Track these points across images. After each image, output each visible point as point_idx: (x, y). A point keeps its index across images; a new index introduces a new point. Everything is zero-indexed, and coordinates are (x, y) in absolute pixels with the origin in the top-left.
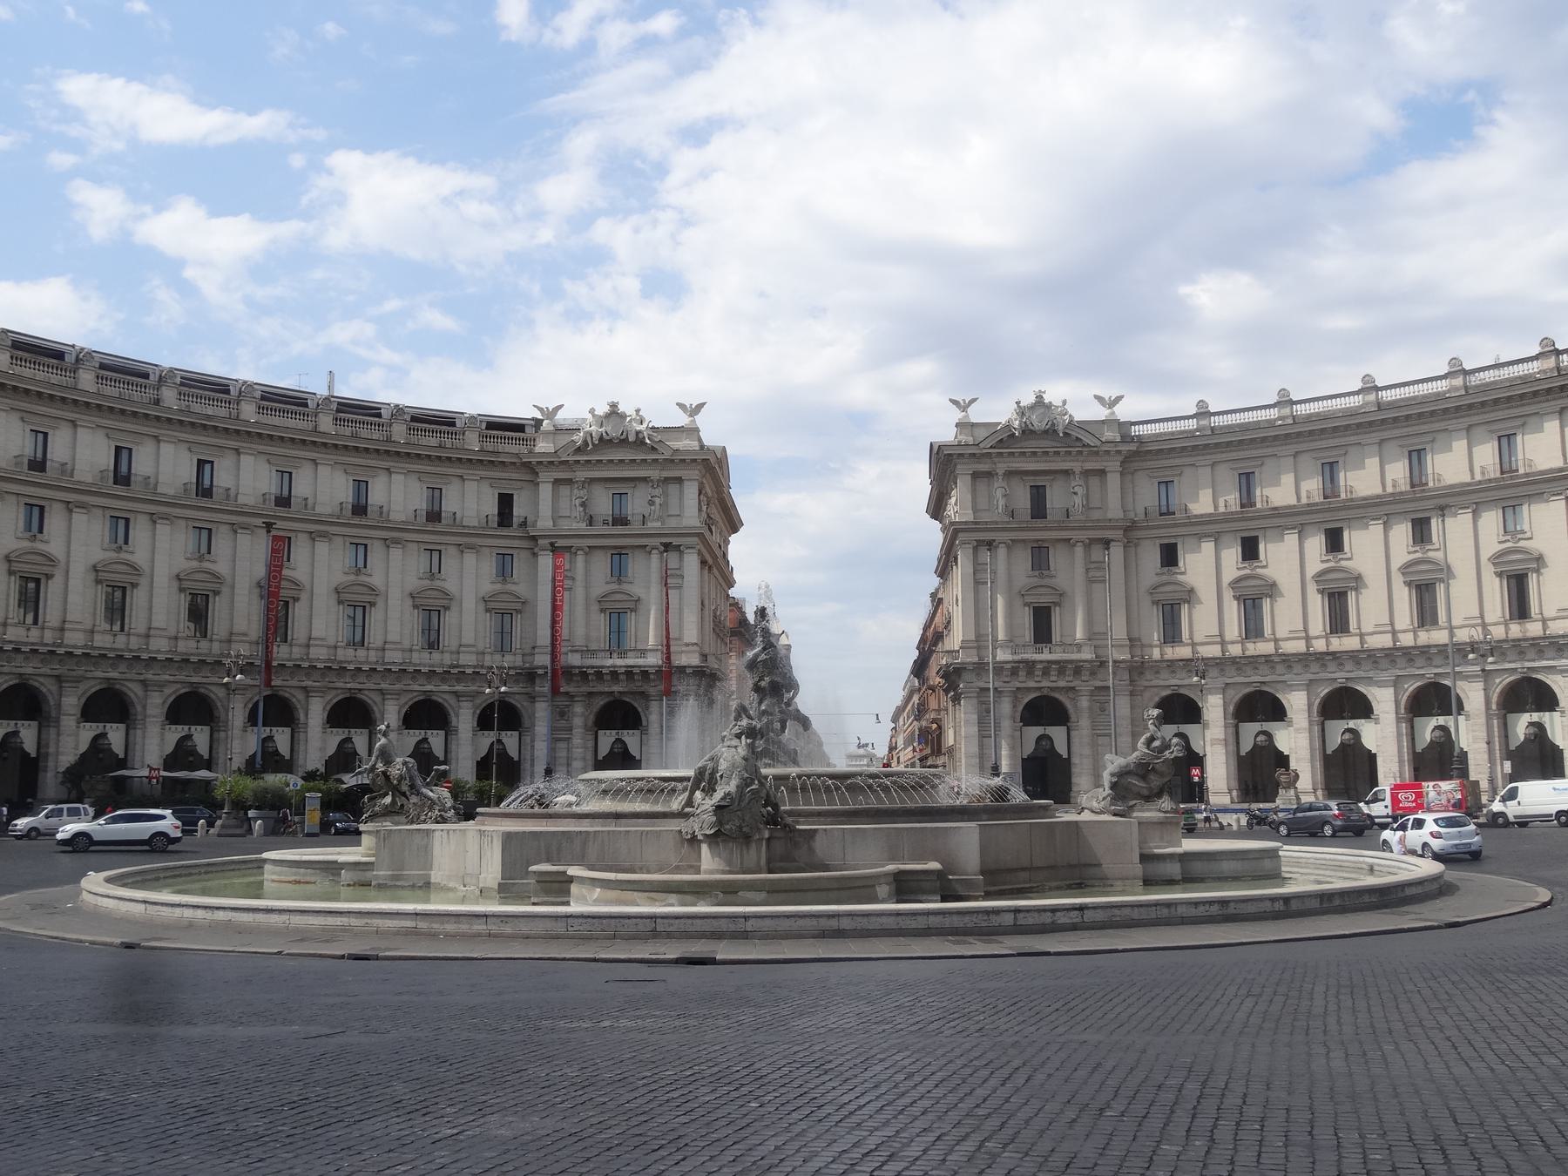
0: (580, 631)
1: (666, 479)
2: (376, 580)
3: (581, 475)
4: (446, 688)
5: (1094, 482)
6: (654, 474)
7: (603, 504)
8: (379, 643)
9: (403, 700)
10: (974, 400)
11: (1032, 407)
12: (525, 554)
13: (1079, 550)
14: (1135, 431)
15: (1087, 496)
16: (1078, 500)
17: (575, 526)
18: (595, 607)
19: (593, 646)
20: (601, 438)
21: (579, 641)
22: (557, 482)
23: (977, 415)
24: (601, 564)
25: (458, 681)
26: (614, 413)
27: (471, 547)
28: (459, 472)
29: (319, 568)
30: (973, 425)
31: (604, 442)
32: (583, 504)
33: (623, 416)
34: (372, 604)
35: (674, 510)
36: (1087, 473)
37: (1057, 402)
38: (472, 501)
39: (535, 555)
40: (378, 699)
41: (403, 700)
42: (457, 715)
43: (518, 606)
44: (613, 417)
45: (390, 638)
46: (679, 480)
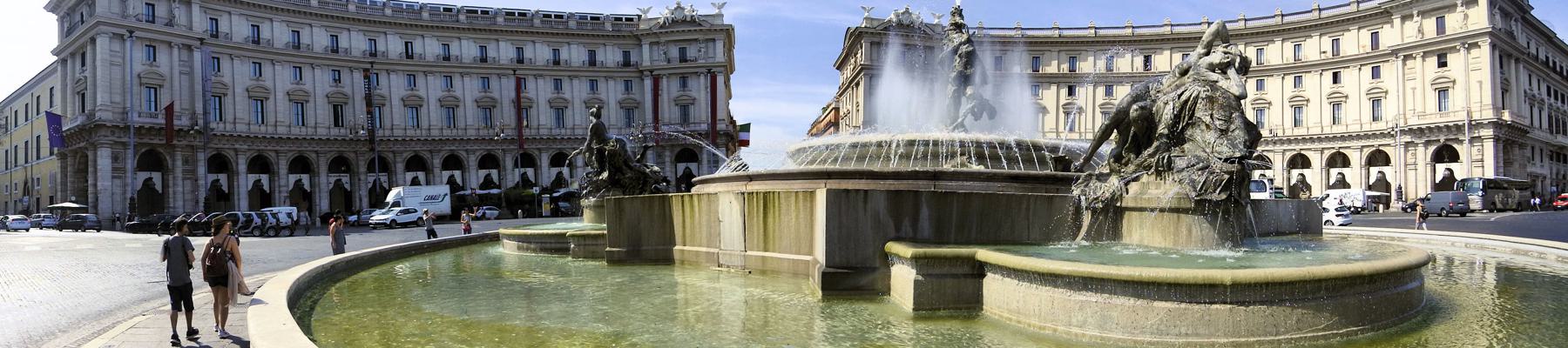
0: (666, 116)
2: (567, 96)
3: (663, 39)
29: (540, 91)
31: (674, 22)
38: (610, 56)
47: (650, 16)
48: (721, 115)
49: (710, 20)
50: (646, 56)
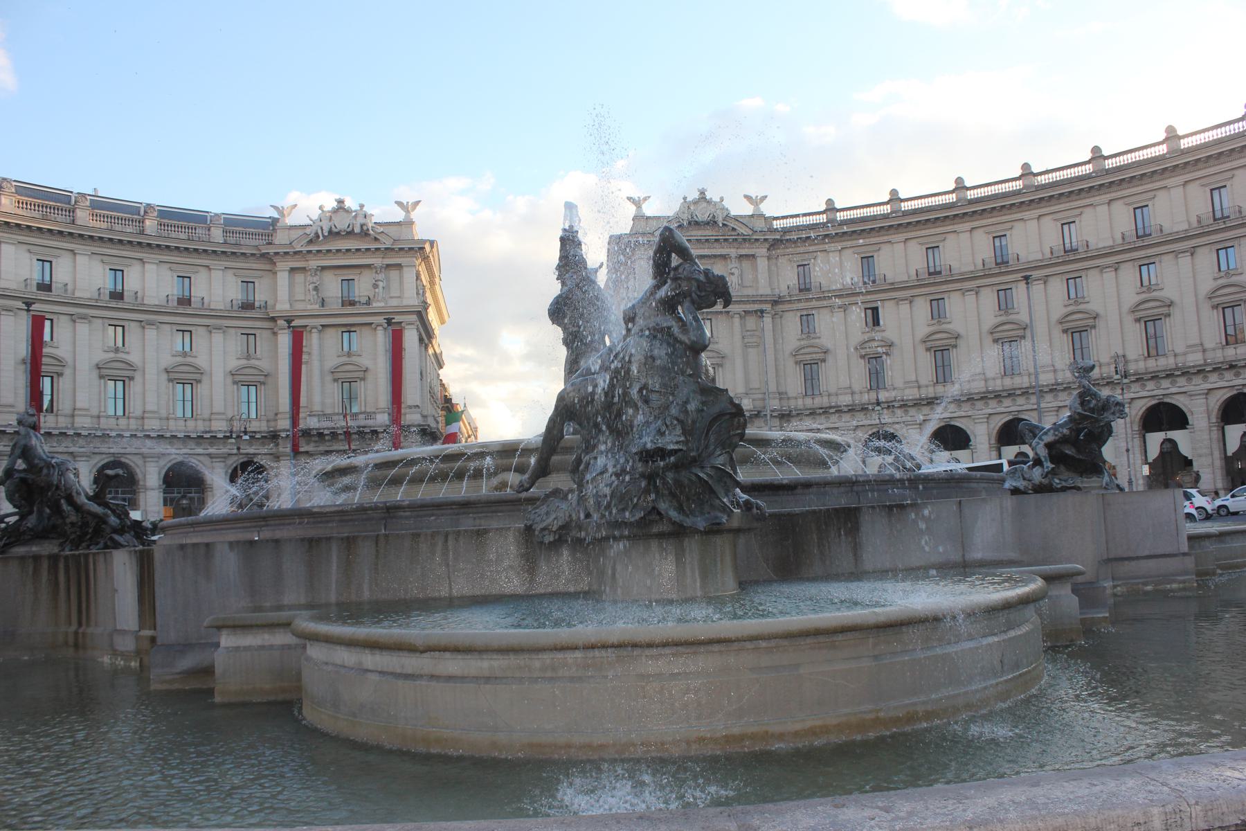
0: (317, 398)
1: (388, 266)
2: (134, 358)
4: (200, 451)
5: (746, 264)
6: (377, 261)
7: (332, 286)
8: (138, 413)
9: (162, 462)
10: (645, 199)
11: (695, 202)
12: (266, 334)
13: (737, 320)
14: (777, 224)
15: (741, 275)
17: (309, 307)
18: (329, 378)
19: (328, 411)
20: (330, 232)
21: (317, 408)
22: (293, 270)
23: (649, 210)
25: (212, 445)
29: (78, 345)
30: (648, 218)
32: (316, 289)
33: (348, 211)
34: (131, 378)
39: (275, 334)
40: (140, 462)
41: (162, 462)
43: (262, 379)
44: (341, 213)
45: (149, 407)
46: (399, 266)
47: (290, 221)
48: (411, 394)
49: (392, 231)
50: (283, 292)
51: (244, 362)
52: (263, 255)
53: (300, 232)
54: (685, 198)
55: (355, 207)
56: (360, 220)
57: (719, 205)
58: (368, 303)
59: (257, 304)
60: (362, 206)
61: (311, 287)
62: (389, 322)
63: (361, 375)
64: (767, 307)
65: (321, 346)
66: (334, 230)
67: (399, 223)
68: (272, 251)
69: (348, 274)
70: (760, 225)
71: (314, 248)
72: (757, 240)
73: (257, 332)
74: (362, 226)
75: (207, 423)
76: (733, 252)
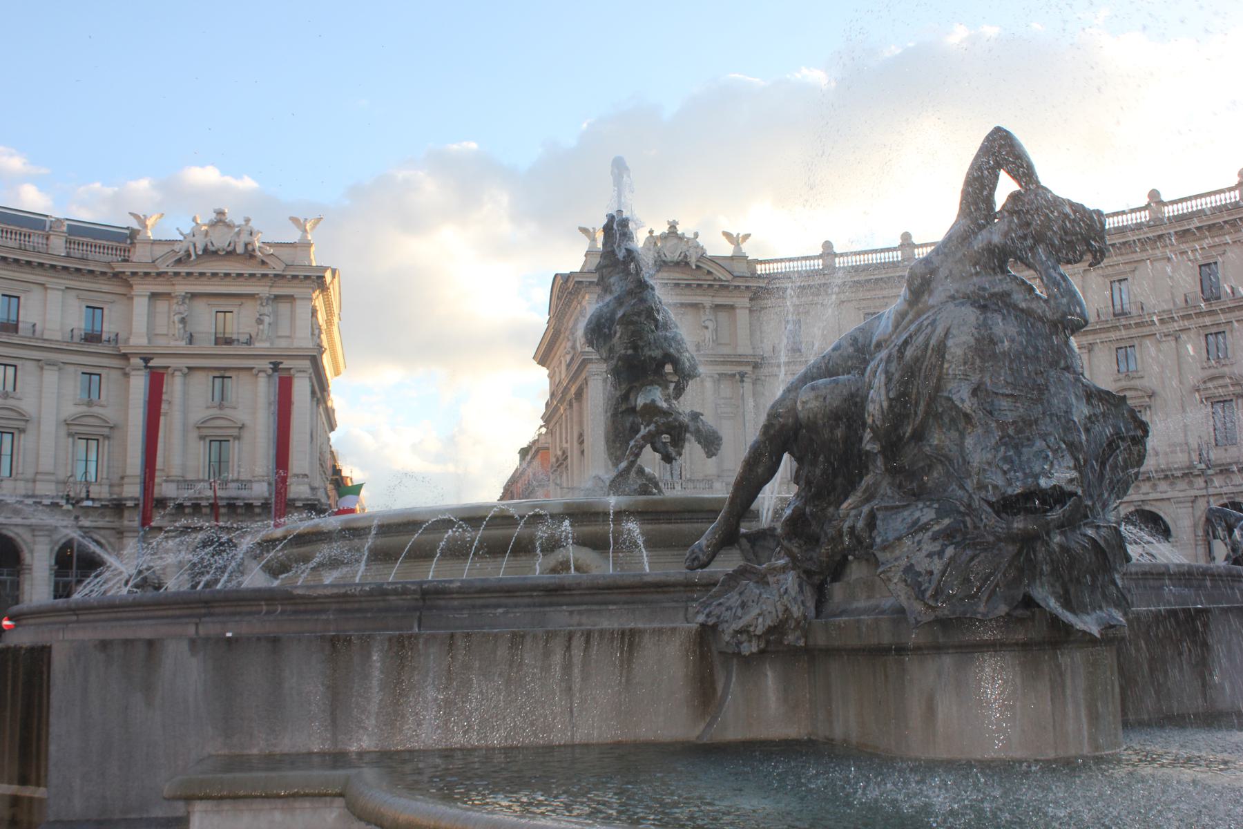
0: (176, 460)
1: (277, 297)
4: (18, 520)
5: (723, 316)
6: (263, 290)
11: (664, 237)
12: (115, 375)
13: (709, 384)
14: (761, 269)
16: (708, 334)
17: (173, 343)
18: (194, 435)
19: (191, 476)
20: (205, 250)
21: (176, 472)
22: (154, 296)
24: (201, 386)
26: (220, 220)
27: (52, 364)
28: (41, 279)
32: (183, 321)
33: (229, 226)
35: (284, 330)
36: (718, 307)
37: (690, 235)
39: (126, 375)
42: (32, 551)
43: (106, 431)
44: (220, 227)
46: (291, 298)
48: (299, 460)
49: (285, 254)
50: (139, 322)
51: (83, 409)
52: (116, 275)
53: (167, 249)
54: (651, 232)
55: (239, 221)
56: (244, 238)
57: (692, 243)
58: (249, 341)
59: (105, 337)
60: (247, 220)
61: (177, 318)
62: (276, 367)
63: (235, 432)
64: (748, 369)
65: (185, 393)
66: (211, 248)
67: (292, 245)
68: (128, 269)
69: (224, 304)
70: (740, 269)
71: (183, 269)
72: (737, 287)
73: (104, 372)
74: (246, 245)
75: (30, 485)
76: (707, 301)
